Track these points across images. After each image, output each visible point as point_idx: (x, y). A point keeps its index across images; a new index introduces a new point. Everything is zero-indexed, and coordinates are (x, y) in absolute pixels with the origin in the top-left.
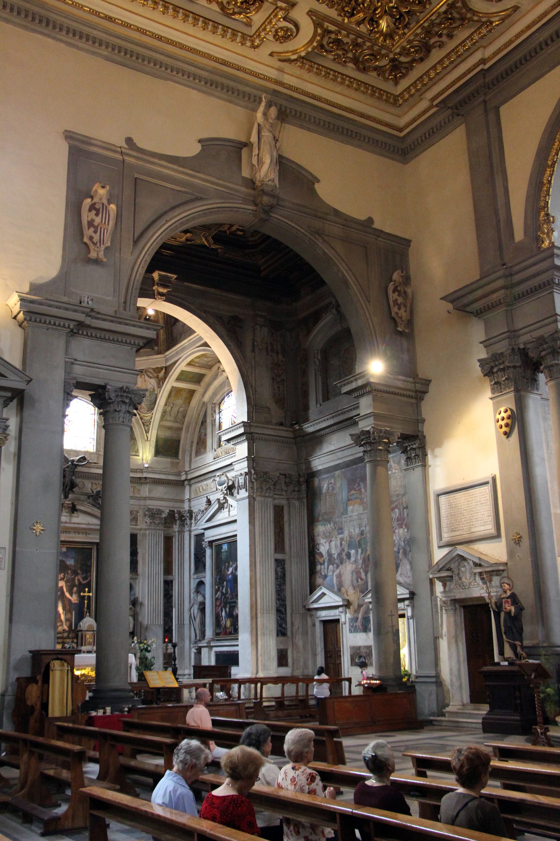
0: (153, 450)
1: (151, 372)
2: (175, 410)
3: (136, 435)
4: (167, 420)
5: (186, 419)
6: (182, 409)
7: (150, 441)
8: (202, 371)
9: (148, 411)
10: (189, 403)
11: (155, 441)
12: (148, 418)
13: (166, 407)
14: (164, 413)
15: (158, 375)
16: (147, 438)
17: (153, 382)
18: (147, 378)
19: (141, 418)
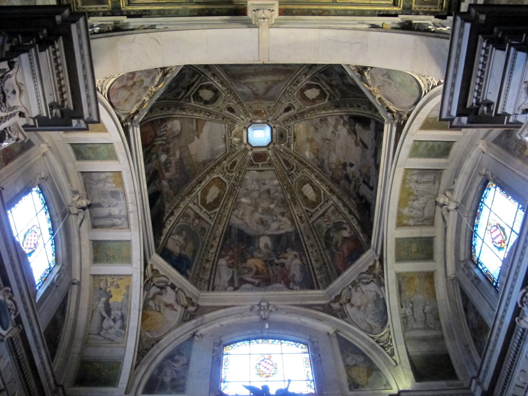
0: (411, 374)
1: (365, 278)
2: (419, 311)
3: (378, 365)
4: (414, 329)
5: (442, 321)
6: (427, 308)
7: (400, 362)
8: (425, 232)
9: (383, 328)
10: (435, 296)
11: (407, 360)
12: (386, 336)
13: (404, 309)
14: (405, 319)
15: (374, 274)
16: (396, 362)
17: (373, 286)
18: (364, 288)
19: (377, 342)
